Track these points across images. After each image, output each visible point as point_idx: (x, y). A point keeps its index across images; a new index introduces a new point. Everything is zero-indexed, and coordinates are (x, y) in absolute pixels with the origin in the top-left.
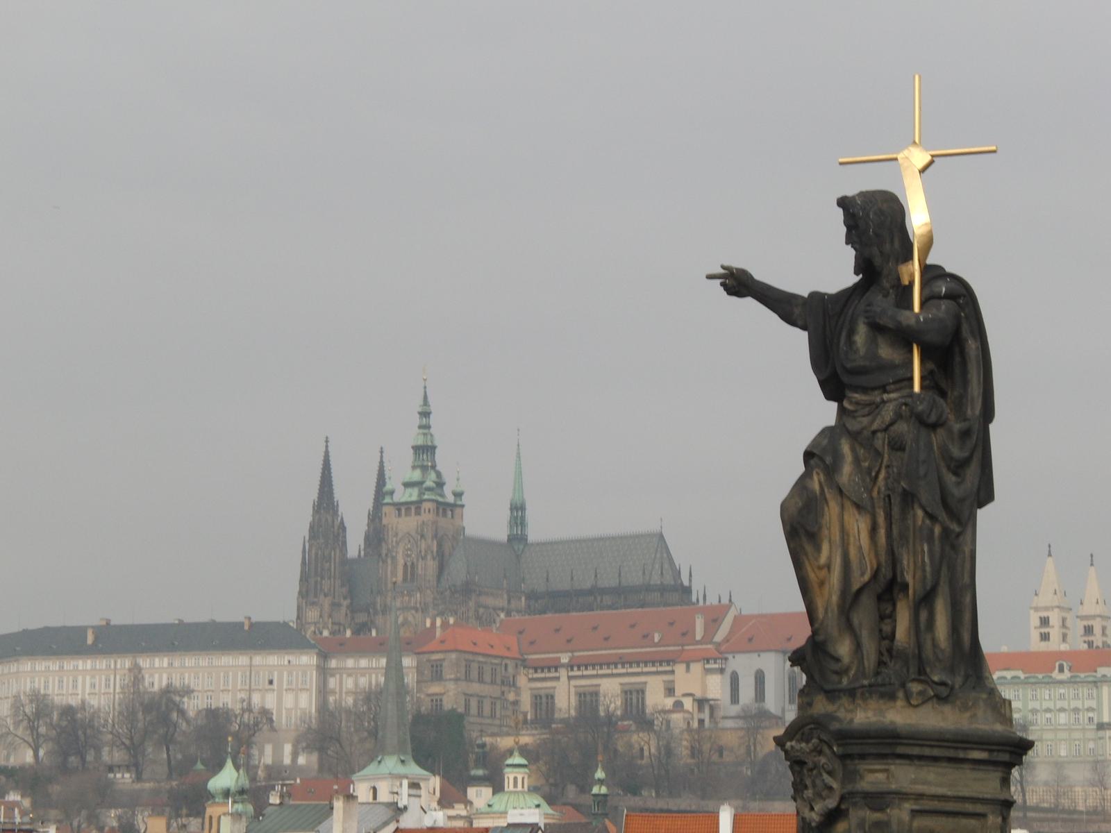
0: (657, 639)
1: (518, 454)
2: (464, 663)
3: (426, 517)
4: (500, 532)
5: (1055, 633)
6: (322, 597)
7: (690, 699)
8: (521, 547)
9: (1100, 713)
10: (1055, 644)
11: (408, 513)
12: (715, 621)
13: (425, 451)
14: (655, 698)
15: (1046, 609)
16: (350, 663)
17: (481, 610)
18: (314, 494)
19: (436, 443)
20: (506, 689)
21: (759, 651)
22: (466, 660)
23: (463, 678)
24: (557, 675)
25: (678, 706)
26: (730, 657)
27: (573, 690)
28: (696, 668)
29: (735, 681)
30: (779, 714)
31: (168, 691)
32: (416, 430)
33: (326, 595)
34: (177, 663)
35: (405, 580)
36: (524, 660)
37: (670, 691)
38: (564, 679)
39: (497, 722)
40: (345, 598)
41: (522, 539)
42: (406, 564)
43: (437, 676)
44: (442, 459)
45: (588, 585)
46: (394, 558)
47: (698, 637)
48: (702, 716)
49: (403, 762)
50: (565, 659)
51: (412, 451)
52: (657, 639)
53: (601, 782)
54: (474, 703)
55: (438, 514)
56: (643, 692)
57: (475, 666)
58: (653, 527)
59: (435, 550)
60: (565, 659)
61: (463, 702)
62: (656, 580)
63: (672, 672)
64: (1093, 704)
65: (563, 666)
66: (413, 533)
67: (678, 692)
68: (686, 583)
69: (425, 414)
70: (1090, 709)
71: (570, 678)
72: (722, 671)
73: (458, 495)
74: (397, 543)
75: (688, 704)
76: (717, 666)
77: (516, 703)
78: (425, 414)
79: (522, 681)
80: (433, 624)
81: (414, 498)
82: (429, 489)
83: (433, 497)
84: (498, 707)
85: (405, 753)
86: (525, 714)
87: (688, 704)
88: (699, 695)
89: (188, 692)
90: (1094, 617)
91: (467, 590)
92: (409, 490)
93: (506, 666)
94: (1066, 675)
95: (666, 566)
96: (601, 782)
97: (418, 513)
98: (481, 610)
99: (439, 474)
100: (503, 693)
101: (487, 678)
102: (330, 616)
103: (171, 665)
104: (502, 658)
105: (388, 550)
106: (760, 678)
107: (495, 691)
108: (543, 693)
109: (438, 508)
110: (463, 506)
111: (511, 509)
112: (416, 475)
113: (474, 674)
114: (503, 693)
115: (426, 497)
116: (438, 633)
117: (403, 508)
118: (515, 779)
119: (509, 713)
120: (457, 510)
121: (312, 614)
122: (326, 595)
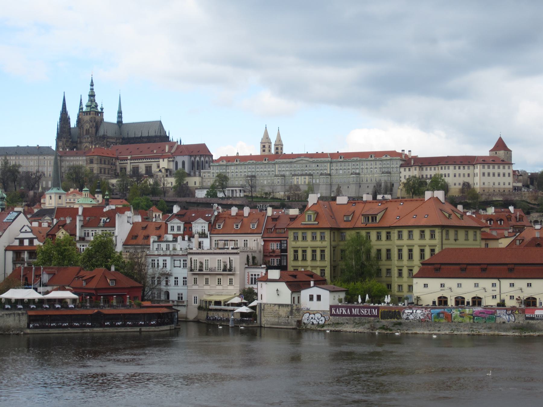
0: (155, 152)
1: (120, 97)
2: (99, 159)
3: (91, 116)
4: (115, 120)
5: (267, 149)
6: (63, 139)
7: (164, 169)
8: (121, 124)
9: (275, 173)
10: (267, 153)
11: (87, 115)
12: (171, 147)
13: (92, 96)
14: (154, 169)
15: (265, 143)
16: (68, 158)
17: (108, 143)
18: (60, 109)
19: (95, 94)
20: (112, 166)
21: (183, 155)
22: (100, 158)
23: (99, 163)
24: (127, 162)
25: (160, 171)
26: (175, 157)
27: (131, 166)
28: (166, 160)
29: (177, 164)
30: (189, 173)
31: (14, 166)
32: (90, 90)
33: (64, 138)
34: (17, 158)
35: (86, 134)
36: (118, 158)
37: (158, 167)
38: (129, 164)
39: (110, 175)
40: (70, 139)
41: (122, 122)
42: (86, 130)
43: (92, 162)
44: (97, 99)
45: (139, 136)
46: (83, 128)
47: (167, 151)
48: (167, 174)
49: (58, 189)
50: (129, 157)
51: (88, 96)
52: (155, 152)
53: (107, 195)
54: (103, 171)
55: (96, 115)
56: (151, 167)
57: (103, 160)
58: (158, 119)
59: (95, 125)
60: (129, 157)
61: (99, 170)
62: (159, 134)
63: (159, 161)
64: (272, 169)
65: (129, 159)
66: (89, 121)
67: (161, 167)
68: (168, 135)
69: (92, 85)
70: (273, 171)
71: (131, 163)
72: (173, 161)
73: (102, 109)
74: (84, 123)
75: (163, 170)
76: (171, 160)
77: (116, 170)
78: (92, 85)
79: (118, 163)
80: (92, 147)
81: (89, 110)
82: (93, 108)
83: (94, 110)
84: (110, 171)
85: (59, 187)
86: (118, 173)
87: (163, 170)
88: (166, 168)
89: (20, 166)
90: (278, 145)
91: (104, 137)
92: (87, 108)
93: (112, 159)
94: (266, 162)
95: (162, 130)
96: (107, 195)
97: (90, 114)
98: (108, 143)
99: (96, 103)
100: (111, 167)
101: (107, 163)
102: (65, 144)
103: (16, 159)
104: (111, 157)
105: (81, 125)
106: (183, 163)
107: (109, 167)
108: (123, 167)
109: (95, 113)
110: (103, 112)
111: (118, 114)
112: (89, 104)
113: (103, 162)
114: (111, 167)
115: (92, 110)
116: (92, 150)
117: (86, 113)
118: (85, 194)
119: (113, 173)
120: (102, 114)
121: (60, 144)
122: (64, 138)
